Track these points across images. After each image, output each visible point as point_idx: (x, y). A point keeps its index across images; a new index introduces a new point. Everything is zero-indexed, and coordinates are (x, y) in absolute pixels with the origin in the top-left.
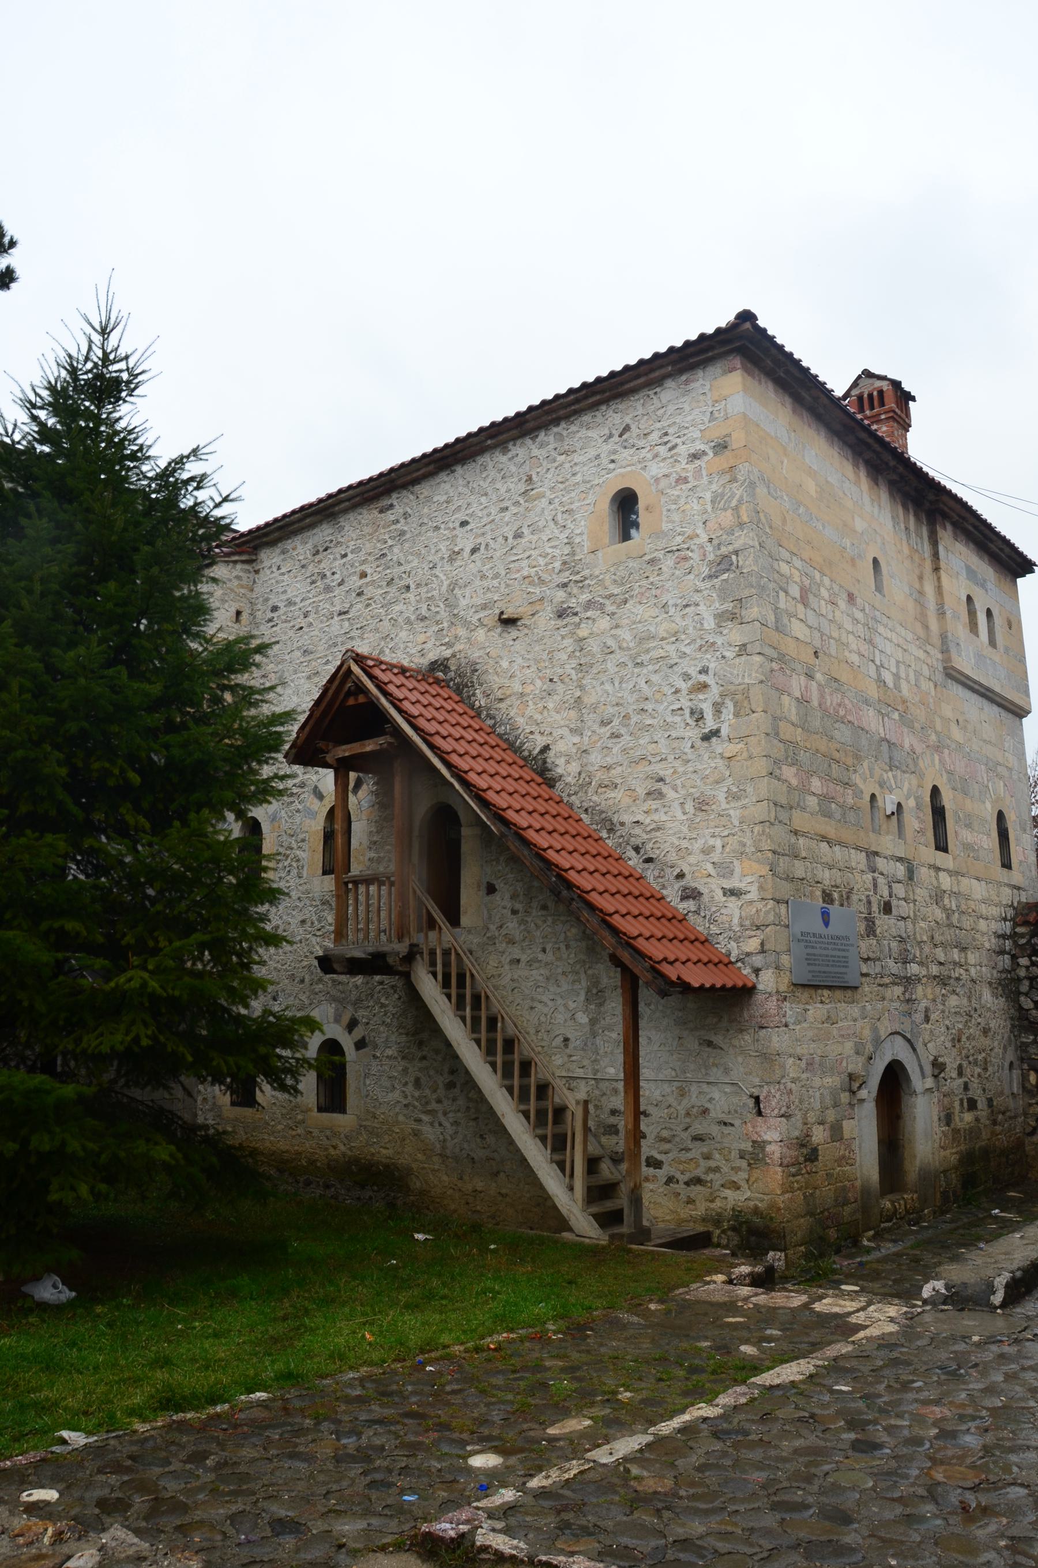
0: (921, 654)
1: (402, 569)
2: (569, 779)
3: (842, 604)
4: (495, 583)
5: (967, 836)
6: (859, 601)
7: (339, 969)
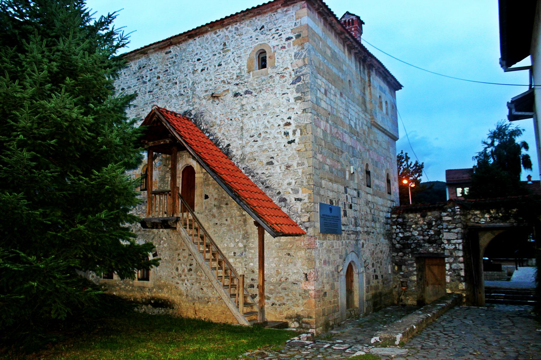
0: (363, 116)
1: (174, 76)
2: (238, 157)
3: (338, 96)
4: (210, 82)
5: (377, 182)
6: (344, 95)
7: (149, 226)
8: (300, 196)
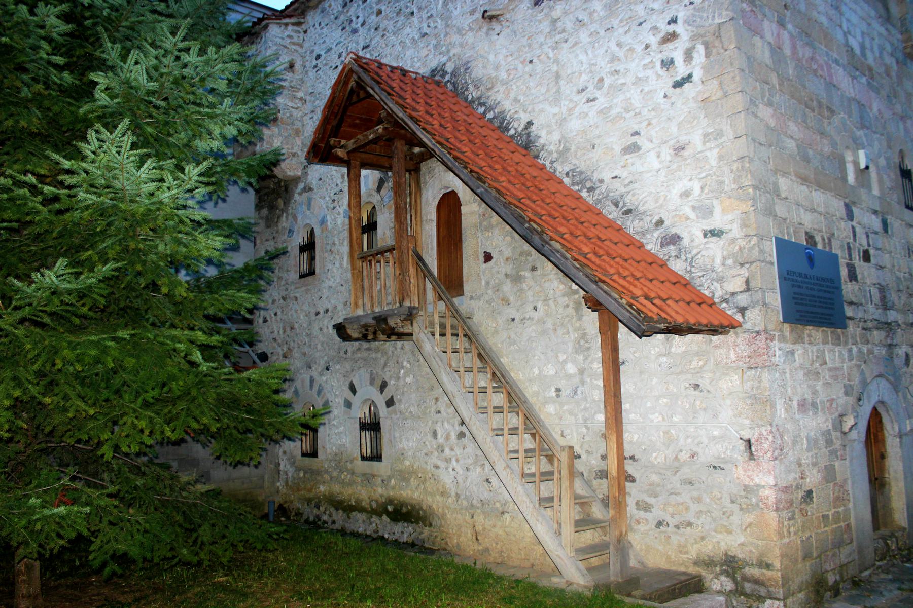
0: (882, 30)
7: (355, 335)
8: (717, 221)
